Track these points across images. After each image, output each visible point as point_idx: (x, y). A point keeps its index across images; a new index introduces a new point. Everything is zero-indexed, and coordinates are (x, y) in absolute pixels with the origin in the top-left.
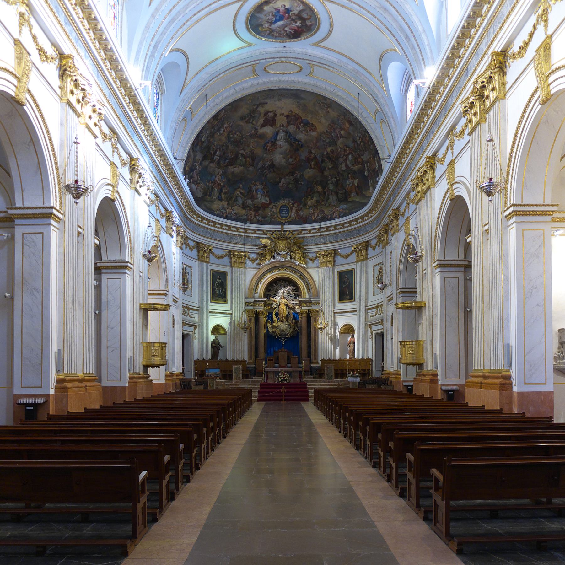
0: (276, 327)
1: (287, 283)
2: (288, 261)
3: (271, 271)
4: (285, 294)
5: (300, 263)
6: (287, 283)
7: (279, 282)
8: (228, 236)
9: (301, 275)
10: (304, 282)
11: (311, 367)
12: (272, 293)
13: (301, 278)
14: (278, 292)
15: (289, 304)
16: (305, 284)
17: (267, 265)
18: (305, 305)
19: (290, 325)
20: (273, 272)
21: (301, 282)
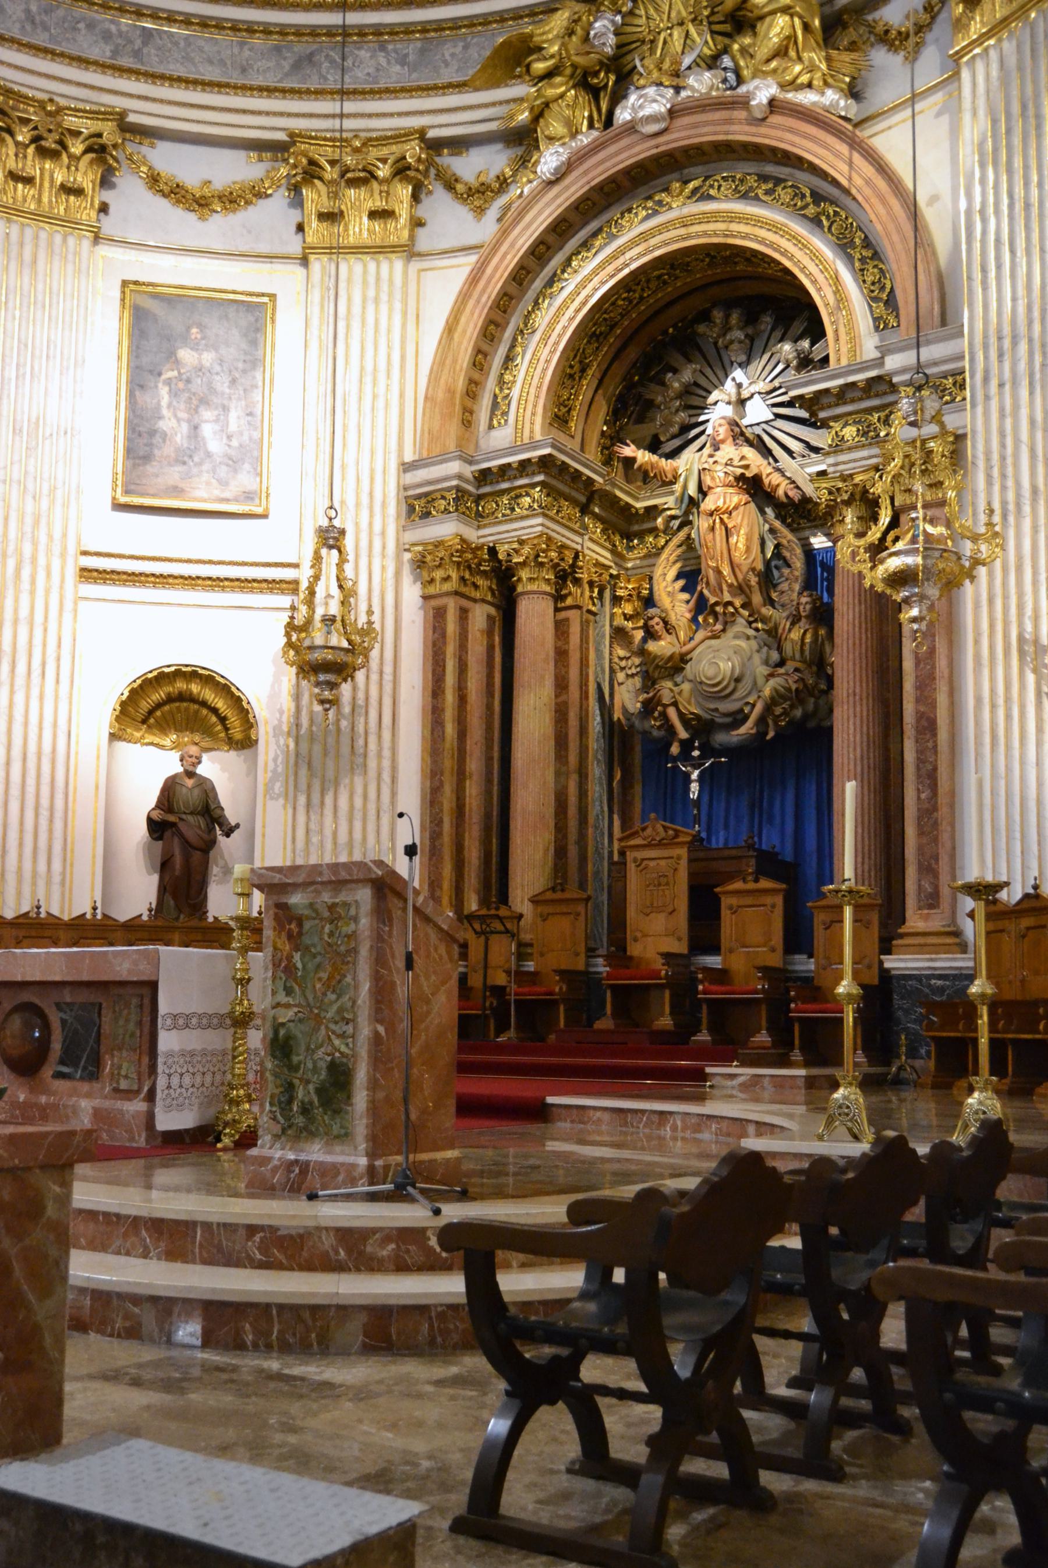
0: (677, 665)
1: (767, 321)
2: (704, 105)
3: (595, 235)
4: (758, 412)
5: (792, 85)
6: (767, 321)
7: (701, 328)
8: (278, 49)
9: (818, 197)
10: (844, 246)
11: (885, 975)
12: (668, 423)
13: (816, 221)
14: (702, 408)
15: (772, 479)
16: (849, 259)
17: (551, 183)
18: (850, 432)
19: (774, 636)
20: (613, 237)
21: (815, 256)
